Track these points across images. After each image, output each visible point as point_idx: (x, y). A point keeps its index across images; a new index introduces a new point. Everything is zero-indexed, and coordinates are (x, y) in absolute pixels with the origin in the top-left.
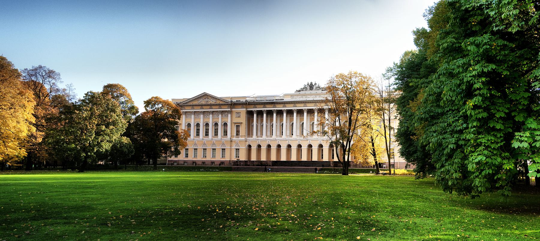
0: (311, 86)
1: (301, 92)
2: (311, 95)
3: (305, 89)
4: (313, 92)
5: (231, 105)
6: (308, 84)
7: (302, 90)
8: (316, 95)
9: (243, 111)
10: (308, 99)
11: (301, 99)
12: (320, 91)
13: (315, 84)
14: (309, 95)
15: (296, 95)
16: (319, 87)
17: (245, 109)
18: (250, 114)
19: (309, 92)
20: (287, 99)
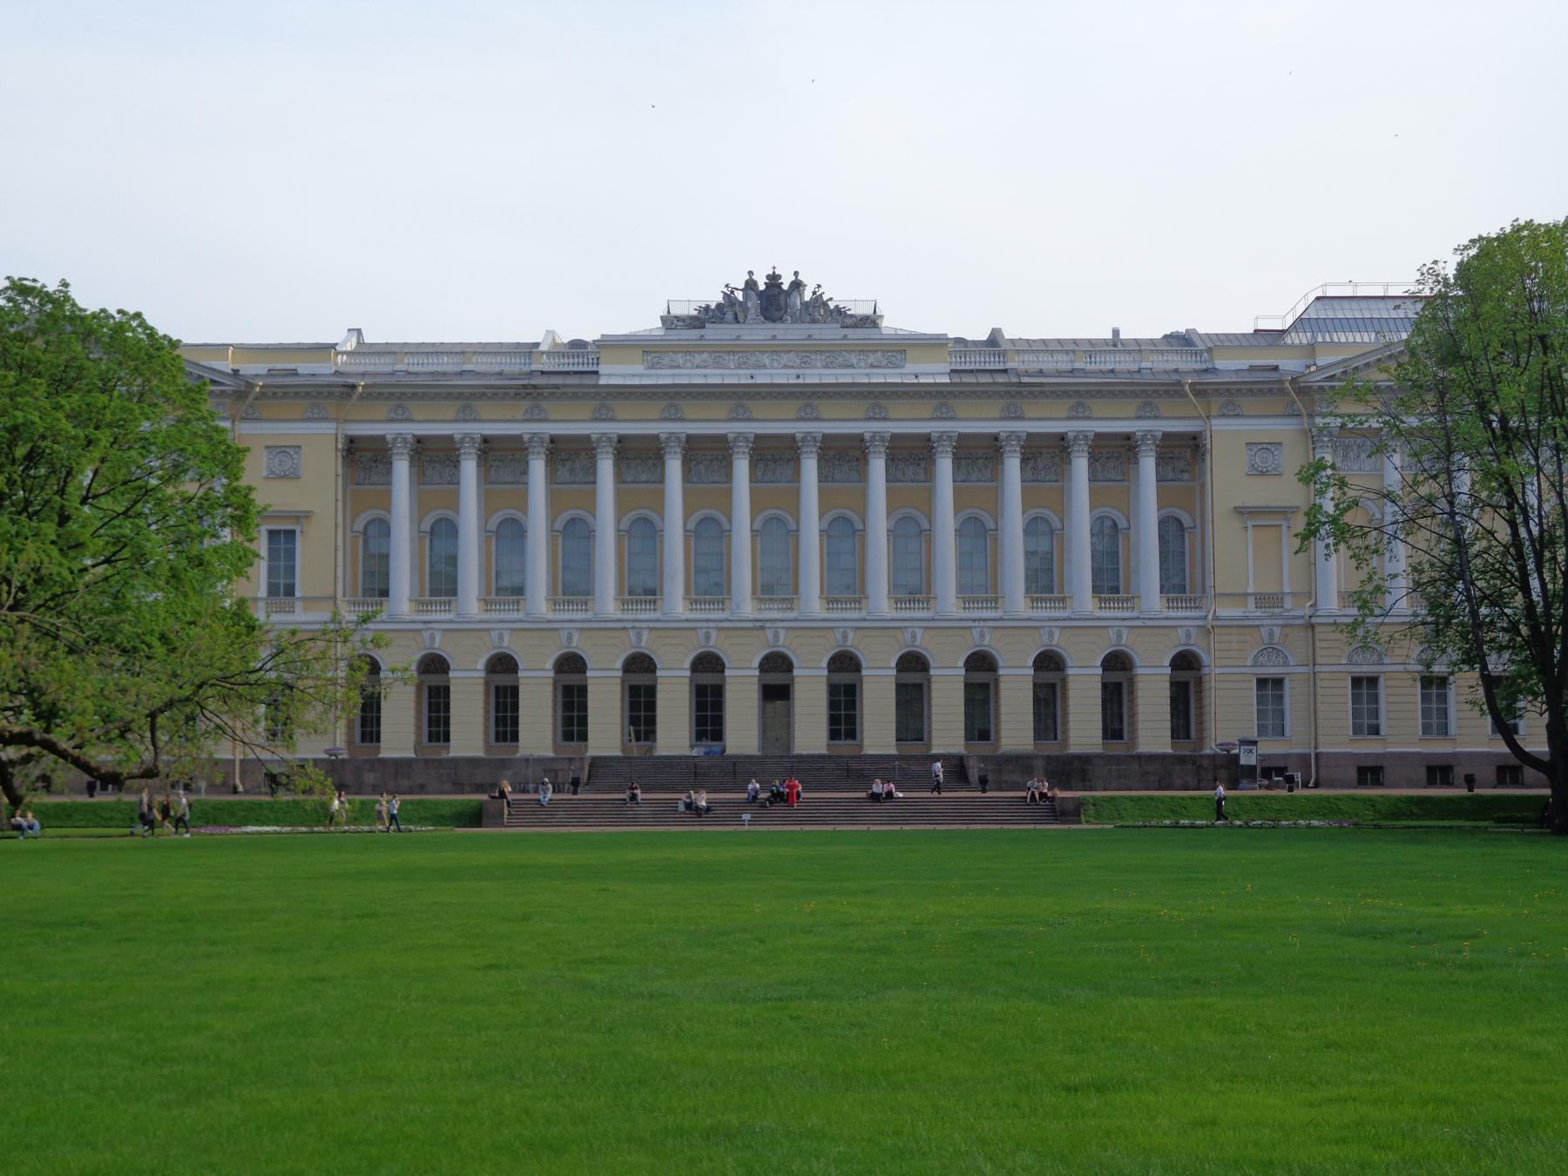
0: (773, 299)
1: (713, 333)
2: (775, 349)
3: (726, 311)
4: (788, 332)
5: (240, 395)
6: (750, 285)
7: (706, 317)
8: (807, 352)
9: (319, 441)
10: (762, 378)
11: (714, 377)
12: (829, 332)
13: (797, 285)
14: (762, 349)
15: (675, 349)
16: (818, 301)
17: (328, 428)
18: (364, 457)
19: (757, 332)
20: (614, 373)
